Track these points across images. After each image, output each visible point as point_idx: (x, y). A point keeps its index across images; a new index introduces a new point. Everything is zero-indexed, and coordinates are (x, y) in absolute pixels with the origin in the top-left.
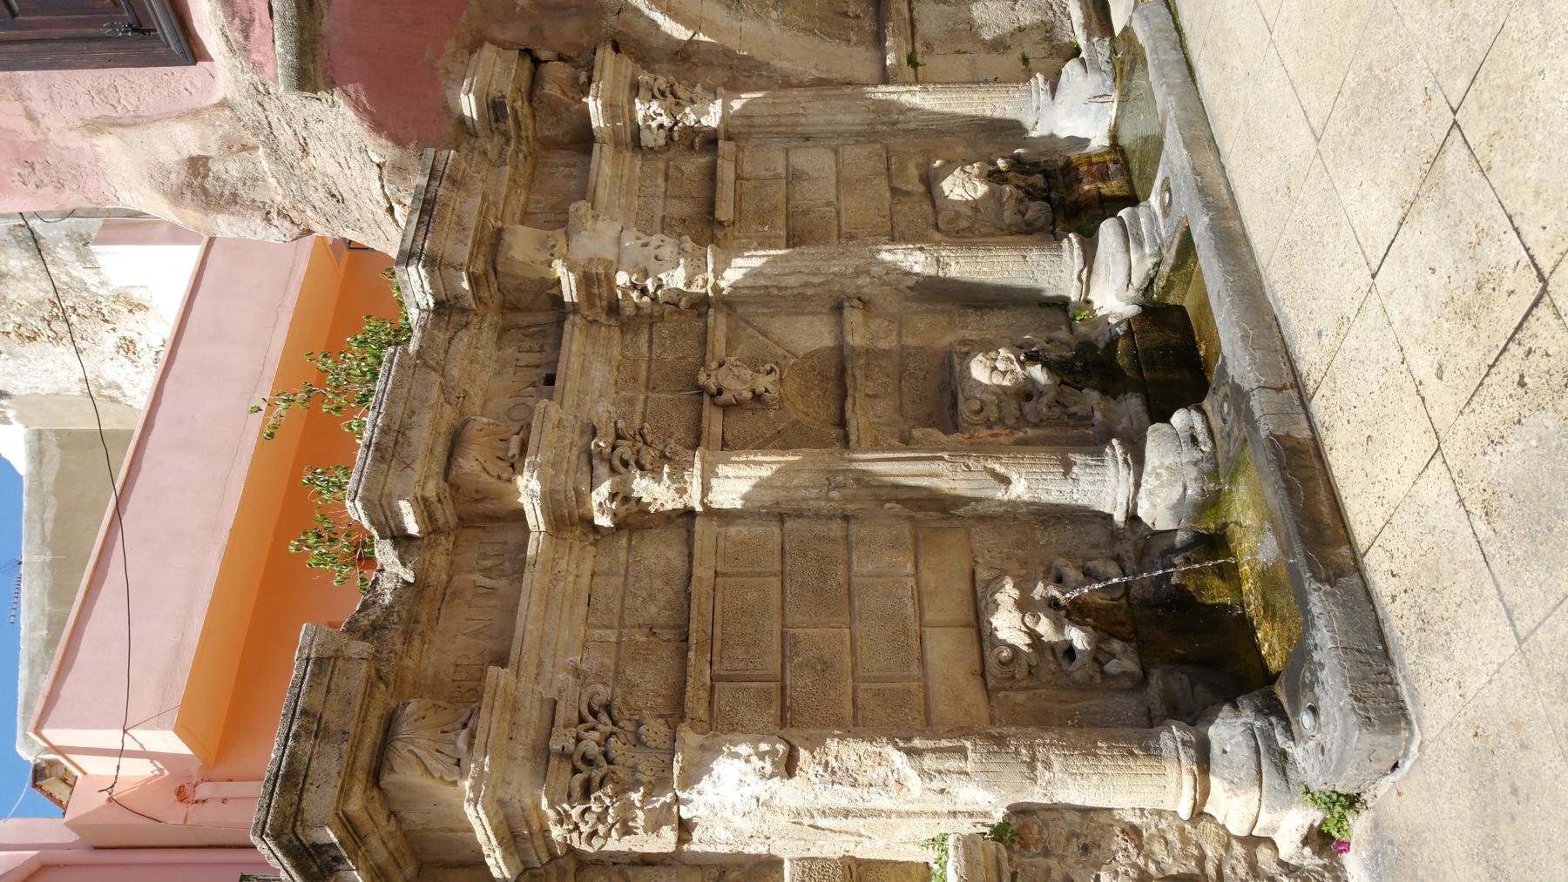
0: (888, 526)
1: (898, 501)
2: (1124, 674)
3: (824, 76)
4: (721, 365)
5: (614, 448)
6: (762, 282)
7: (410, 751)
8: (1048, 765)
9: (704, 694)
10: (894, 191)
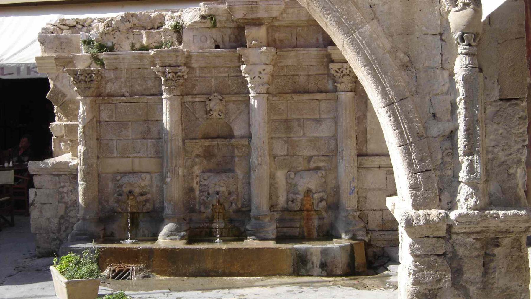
4: (221, 100)
8: (83, 184)
10: (311, 157)
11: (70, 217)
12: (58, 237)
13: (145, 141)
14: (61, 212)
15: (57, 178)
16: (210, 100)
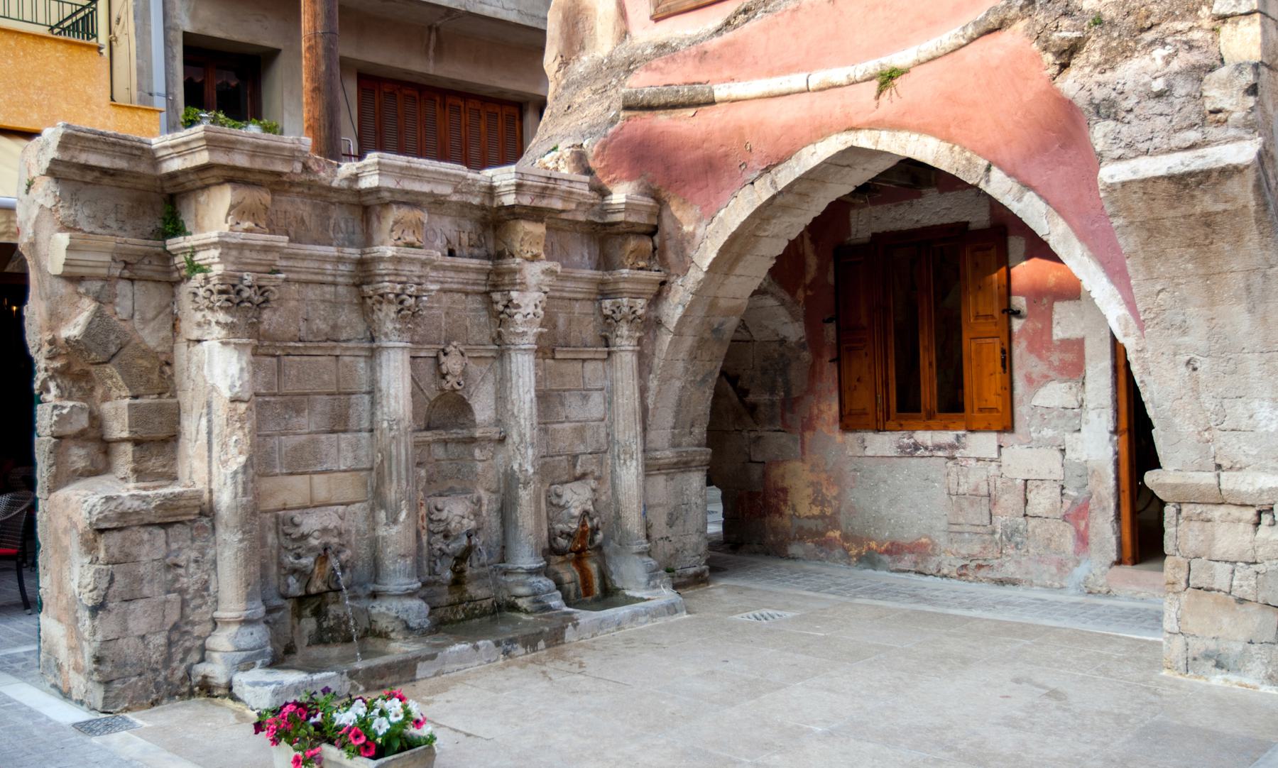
0: (367, 455)
1: (382, 461)
2: (288, 586)
5: (410, 296)
6: (514, 379)
11: (193, 624)
12: (166, 678)
13: (334, 436)
14: (173, 616)
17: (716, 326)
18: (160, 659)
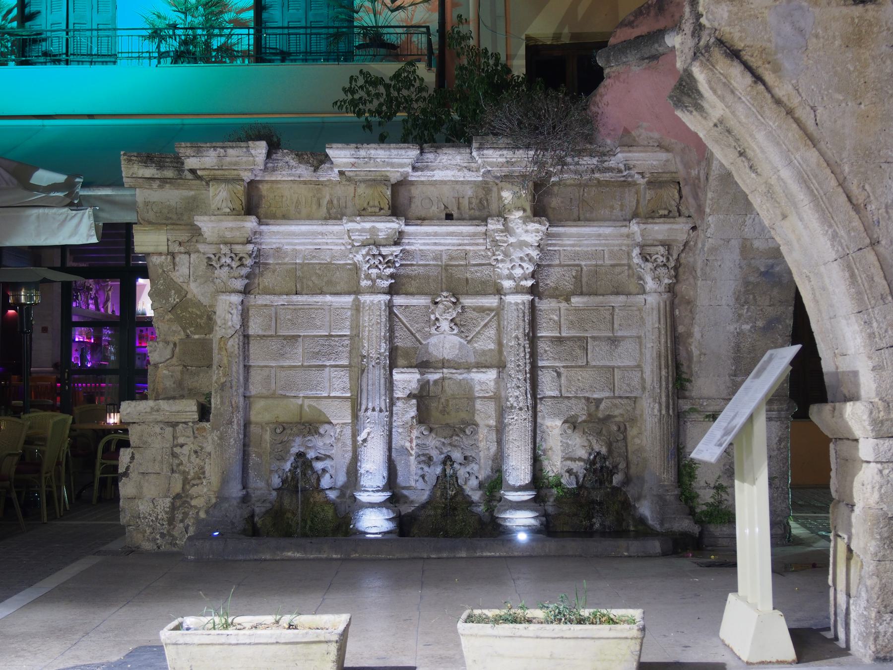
3: (695, 359)
4: (454, 303)
7: (220, 191)
9: (268, 303)
14: (177, 488)
15: (171, 429)
16: (436, 303)
17: (762, 269)
18: (165, 516)
